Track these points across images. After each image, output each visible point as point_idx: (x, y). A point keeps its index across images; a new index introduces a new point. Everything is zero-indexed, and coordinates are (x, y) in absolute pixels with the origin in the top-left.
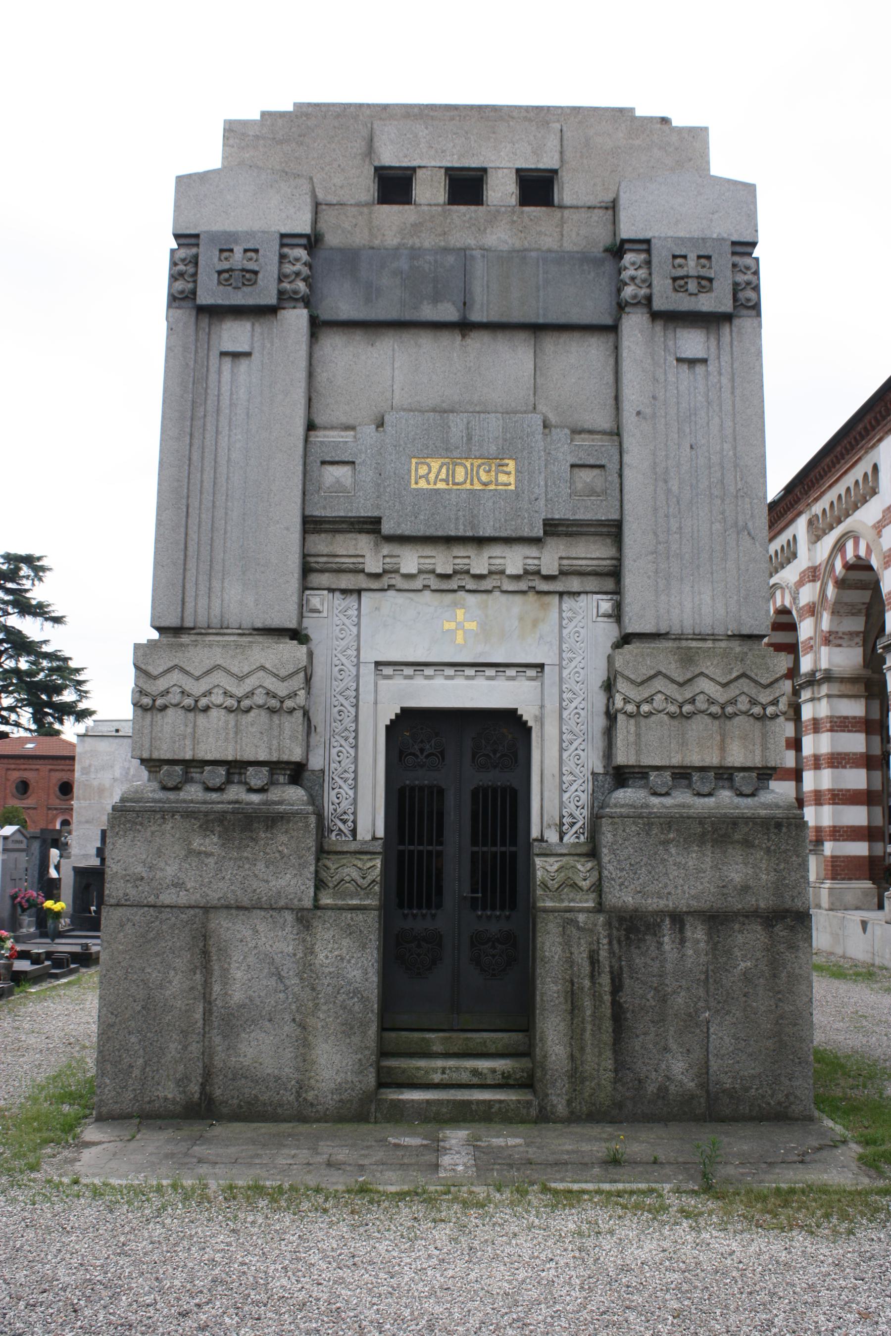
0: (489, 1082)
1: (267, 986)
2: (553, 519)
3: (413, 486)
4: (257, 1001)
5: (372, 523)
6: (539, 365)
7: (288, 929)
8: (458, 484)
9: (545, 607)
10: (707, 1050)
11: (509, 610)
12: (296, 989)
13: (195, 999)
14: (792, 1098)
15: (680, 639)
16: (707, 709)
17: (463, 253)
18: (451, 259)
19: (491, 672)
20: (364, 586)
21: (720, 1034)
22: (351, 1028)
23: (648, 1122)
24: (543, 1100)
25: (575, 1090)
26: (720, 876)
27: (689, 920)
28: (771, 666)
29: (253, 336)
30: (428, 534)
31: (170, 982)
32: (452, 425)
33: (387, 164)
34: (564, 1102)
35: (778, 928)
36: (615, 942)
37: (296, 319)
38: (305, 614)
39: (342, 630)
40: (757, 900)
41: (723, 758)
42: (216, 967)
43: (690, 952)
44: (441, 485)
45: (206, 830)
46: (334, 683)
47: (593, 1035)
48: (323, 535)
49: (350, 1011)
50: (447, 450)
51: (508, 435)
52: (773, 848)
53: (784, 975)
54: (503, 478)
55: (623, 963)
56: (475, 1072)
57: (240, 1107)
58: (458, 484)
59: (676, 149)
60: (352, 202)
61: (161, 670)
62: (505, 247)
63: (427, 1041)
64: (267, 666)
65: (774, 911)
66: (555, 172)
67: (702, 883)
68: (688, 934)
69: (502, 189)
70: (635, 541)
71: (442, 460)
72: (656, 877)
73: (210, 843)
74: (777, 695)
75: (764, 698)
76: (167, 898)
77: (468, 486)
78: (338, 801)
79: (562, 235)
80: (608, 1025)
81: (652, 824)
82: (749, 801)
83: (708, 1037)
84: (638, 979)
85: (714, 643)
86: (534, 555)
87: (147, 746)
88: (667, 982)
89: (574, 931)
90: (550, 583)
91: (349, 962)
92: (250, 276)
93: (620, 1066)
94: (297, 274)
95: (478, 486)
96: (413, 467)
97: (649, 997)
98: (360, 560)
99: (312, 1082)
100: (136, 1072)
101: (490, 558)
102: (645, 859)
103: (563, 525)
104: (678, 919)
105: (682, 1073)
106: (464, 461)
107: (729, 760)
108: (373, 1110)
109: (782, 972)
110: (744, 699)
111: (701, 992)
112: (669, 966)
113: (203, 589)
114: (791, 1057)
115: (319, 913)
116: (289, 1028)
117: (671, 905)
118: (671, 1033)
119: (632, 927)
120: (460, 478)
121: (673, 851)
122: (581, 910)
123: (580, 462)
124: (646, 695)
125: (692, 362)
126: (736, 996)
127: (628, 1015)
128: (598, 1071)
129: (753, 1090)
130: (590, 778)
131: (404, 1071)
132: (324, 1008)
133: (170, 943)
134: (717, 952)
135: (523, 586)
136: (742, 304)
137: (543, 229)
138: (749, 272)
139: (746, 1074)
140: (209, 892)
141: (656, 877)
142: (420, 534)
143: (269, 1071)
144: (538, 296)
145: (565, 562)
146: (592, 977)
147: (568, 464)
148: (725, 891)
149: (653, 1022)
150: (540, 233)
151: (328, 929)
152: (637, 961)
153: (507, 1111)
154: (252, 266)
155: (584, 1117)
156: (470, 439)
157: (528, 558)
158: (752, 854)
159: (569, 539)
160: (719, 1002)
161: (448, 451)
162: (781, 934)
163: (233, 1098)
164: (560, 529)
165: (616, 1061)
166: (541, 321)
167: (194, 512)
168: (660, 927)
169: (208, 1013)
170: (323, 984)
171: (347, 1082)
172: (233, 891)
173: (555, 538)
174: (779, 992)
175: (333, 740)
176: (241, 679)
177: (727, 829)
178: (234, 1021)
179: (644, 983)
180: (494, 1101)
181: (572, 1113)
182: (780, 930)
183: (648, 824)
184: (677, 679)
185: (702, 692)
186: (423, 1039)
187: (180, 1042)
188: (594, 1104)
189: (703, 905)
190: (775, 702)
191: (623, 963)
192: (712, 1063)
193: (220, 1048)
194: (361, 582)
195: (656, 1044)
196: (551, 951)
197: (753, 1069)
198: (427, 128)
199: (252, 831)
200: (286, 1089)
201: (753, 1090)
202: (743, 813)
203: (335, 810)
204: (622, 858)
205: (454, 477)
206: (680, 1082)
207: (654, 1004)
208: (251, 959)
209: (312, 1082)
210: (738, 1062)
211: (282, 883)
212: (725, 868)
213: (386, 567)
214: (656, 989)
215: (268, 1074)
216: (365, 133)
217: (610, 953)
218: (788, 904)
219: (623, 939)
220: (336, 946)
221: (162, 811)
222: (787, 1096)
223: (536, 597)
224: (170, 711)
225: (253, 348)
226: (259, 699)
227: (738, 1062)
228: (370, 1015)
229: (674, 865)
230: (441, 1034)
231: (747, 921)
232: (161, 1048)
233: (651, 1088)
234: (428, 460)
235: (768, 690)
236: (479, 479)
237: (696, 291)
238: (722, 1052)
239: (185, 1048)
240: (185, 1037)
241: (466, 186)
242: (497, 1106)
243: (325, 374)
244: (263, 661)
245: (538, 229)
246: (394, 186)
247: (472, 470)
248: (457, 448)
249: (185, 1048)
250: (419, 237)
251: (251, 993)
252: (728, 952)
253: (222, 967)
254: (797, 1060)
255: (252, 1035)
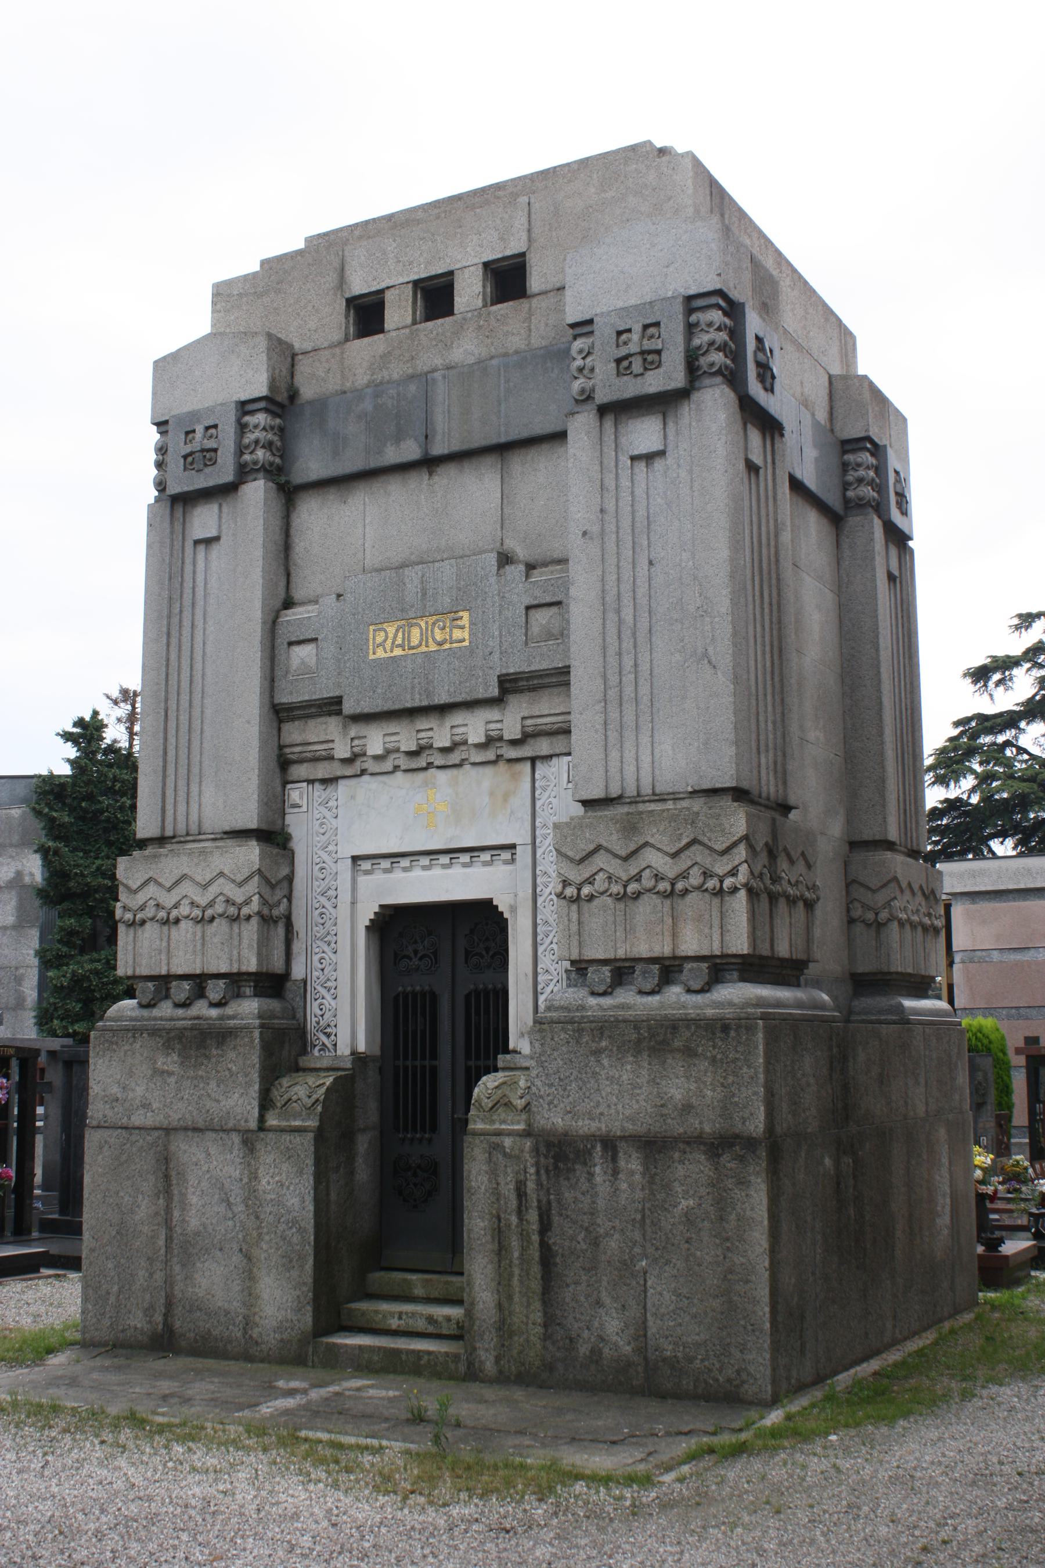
0: (445, 1332)
1: (218, 1213)
2: (508, 675)
3: (372, 657)
4: (210, 1228)
5: (331, 704)
6: (506, 491)
7: (235, 1152)
8: (413, 648)
9: (515, 777)
10: (645, 1307)
11: (479, 783)
12: (243, 1217)
13: (159, 1224)
14: (744, 1376)
15: (636, 802)
16: (655, 887)
17: (425, 379)
18: (413, 388)
19: (465, 858)
20: (339, 773)
21: (659, 1289)
22: (291, 1261)
23: (581, 1390)
24: (471, 1354)
25: (503, 1345)
26: (658, 1093)
27: (622, 1146)
28: (728, 826)
29: (220, 518)
30: (385, 709)
31: (139, 1206)
32: (407, 581)
33: (357, 293)
34: (492, 1359)
35: (725, 1158)
36: (542, 1172)
37: (256, 492)
38: (287, 810)
39: (322, 824)
40: (701, 1123)
41: (675, 946)
42: (176, 1192)
43: (624, 1186)
44: (398, 652)
45: (168, 1047)
46: (316, 883)
47: (521, 1282)
48: (296, 723)
49: (290, 1243)
50: (402, 610)
51: (462, 583)
52: (719, 1057)
53: (733, 1217)
54: (457, 634)
55: (552, 1197)
56: (431, 1320)
57: (196, 1341)
58: (413, 648)
59: (654, 190)
60: (326, 344)
61: (139, 883)
62: (471, 360)
63: (408, 1283)
64: (226, 872)
65: (721, 1137)
66: (523, 255)
67: (637, 1102)
68: (622, 1163)
69: (470, 291)
70: (581, 689)
71: (398, 623)
72: (588, 1094)
73: (169, 1062)
74: (736, 863)
75: (721, 868)
76: (137, 1120)
77: (423, 649)
78: (321, 1013)
79: (530, 330)
80: (536, 1270)
81: (583, 1030)
82: (699, 998)
83: (645, 1291)
84: (567, 1216)
85: (674, 804)
86: (496, 718)
87: (131, 962)
88: (599, 1221)
89: (500, 1157)
90: (518, 748)
91: (288, 1188)
92: (209, 456)
93: (550, 1320)
94: (257, 442)
95: (433, 647)
96: (371, 636)
97: (580, 1239)
98: (331, 745)
99: (257, 1318)
100: (112, 1299)
101: (452, 727)
102: (575, 1073)
103: (522, 679)
104: (610, 1144)
105: (617, 1334)
106: (418, 621)
107: (682, 948)
108: (310, 1353)
109: (731, 1214)
110: (695, 871)
111: (637, 1235)
112: (601, 1203)
113: (182, 794)
114: (742, 1322)
115: (262, 1135)
116: (237, 1259)
117: (604, 1128)
118: (604, 1283)
119: (560, 1153)
120: (415, 641)
121: (606, 1062)
122: (510, 1133)
123: (536, 602)
124: (587, 875)
125: (649, 458)
126: (676, 1242)
127: (558, 1260)
128: (527, 1324)
129: (698, 1362)
130: (564, 976)
131: (363, 1314)
132: (267, 1238)
133: (138, 1166)
134: (655, 1187)
135: (490, 755)
136: (705, 372)
137: (517, 327)
138: (711, 330)
139: (690, 1340)
140: (171, 1114)
141: (588, 1094)
142: (378, 710)
143: (220, 1304)
144: (499, 411)
145: (529, 722)
146: (519, 1212)
147: (523, 607)
148: (665, 1111)
149: (584, 1269)
150: (507, 334)
151: (270, 1153)
152: (567, 1195)
153: (436, 1364)
154: (211, 444)
155: (513, 1378)
156: (424, 594)
157: (490, 722)
158: (695, 1065)
159: (531, 694)
160: (657, 1249)
161: (404, 613)
162: (728, 1165)
163: (190, 1330)
164: (521, 684)
165: (545, 1313)
166: (503, 440)
167: (172, 714)
168: (590, 1154)
169: (169, 1239)
170: (266, 1212)
171: (287, 1321)
172: (190, 1112)
173: (518, 695)
174: (727, 1239)
175: (314, 946)
176: (205, 887)
177: (665, 1034)
178: (191, 1250)
179: (575, 1222)
180: (423, 1351)
181: (501, 1372)
182: (727, 1161)
183: (578, 1030)
184: (619, 853)
185: (649, 867)
186: (405, 1280)
187: (147, 1270)
188: (523, 1364)
189: (639, 1129)
190: (733, 873)
191: (552, 1197)
192: (650, 1323)
193: (178, 1277)
194: (338, 770)
195: (587, 1296)
196: (477, 1181)
197: (698, 1334)
198: (394, 241)
199: (205, 1048)
200: (234, 1324)
201: (698, 1362)
202: (686, 1014)
203: (318, 1023)
204: (551, 1071)
205: (409, 641)
206: (615, 1344)
207: (585, 1247)
208: (204, 1184)
209: (257, 1318)
210: (680, 1325)
211: (231, 1102)
212: (664, 1083)
213: (355, 750)
214: (587, 1229)
215: (219, 1308)
216: (336, 263)
217: (537, 1185)
218: (739, 1128)
219: (551, 1168)
220: (277, 1171)
221: (135, 1030)
222: (738, 1372)
223: (506, 766)
224: (148, 926)
225: (220, 531)
226: (219, 908)
227: (680, 1325)
228: (307, 1247)
229: (607, 1079)
230: (420, 1276)
231: (688, 1149)
232: (131, 1274)
233: (584, 1350)
234: (385, 626)
235: (726, 857)
236: (434, 639)
237: (641, 370)
238: (662, 1310)
239: (151, 1275)
240: (151, 1264)
241: (436, 296)
242: (426, 1357)
243: (302, 544)
244: (222, 867)
245: (506, 329)
246: (367, 314)
247: (427, 629)
248: (412, 606)
249: (151, 1275)
250: (387, 368)
251: (204, 1219)
252: (667, 1187)
253: (180, 1192)
254: (750, 1328)
255: (206, 1265)
